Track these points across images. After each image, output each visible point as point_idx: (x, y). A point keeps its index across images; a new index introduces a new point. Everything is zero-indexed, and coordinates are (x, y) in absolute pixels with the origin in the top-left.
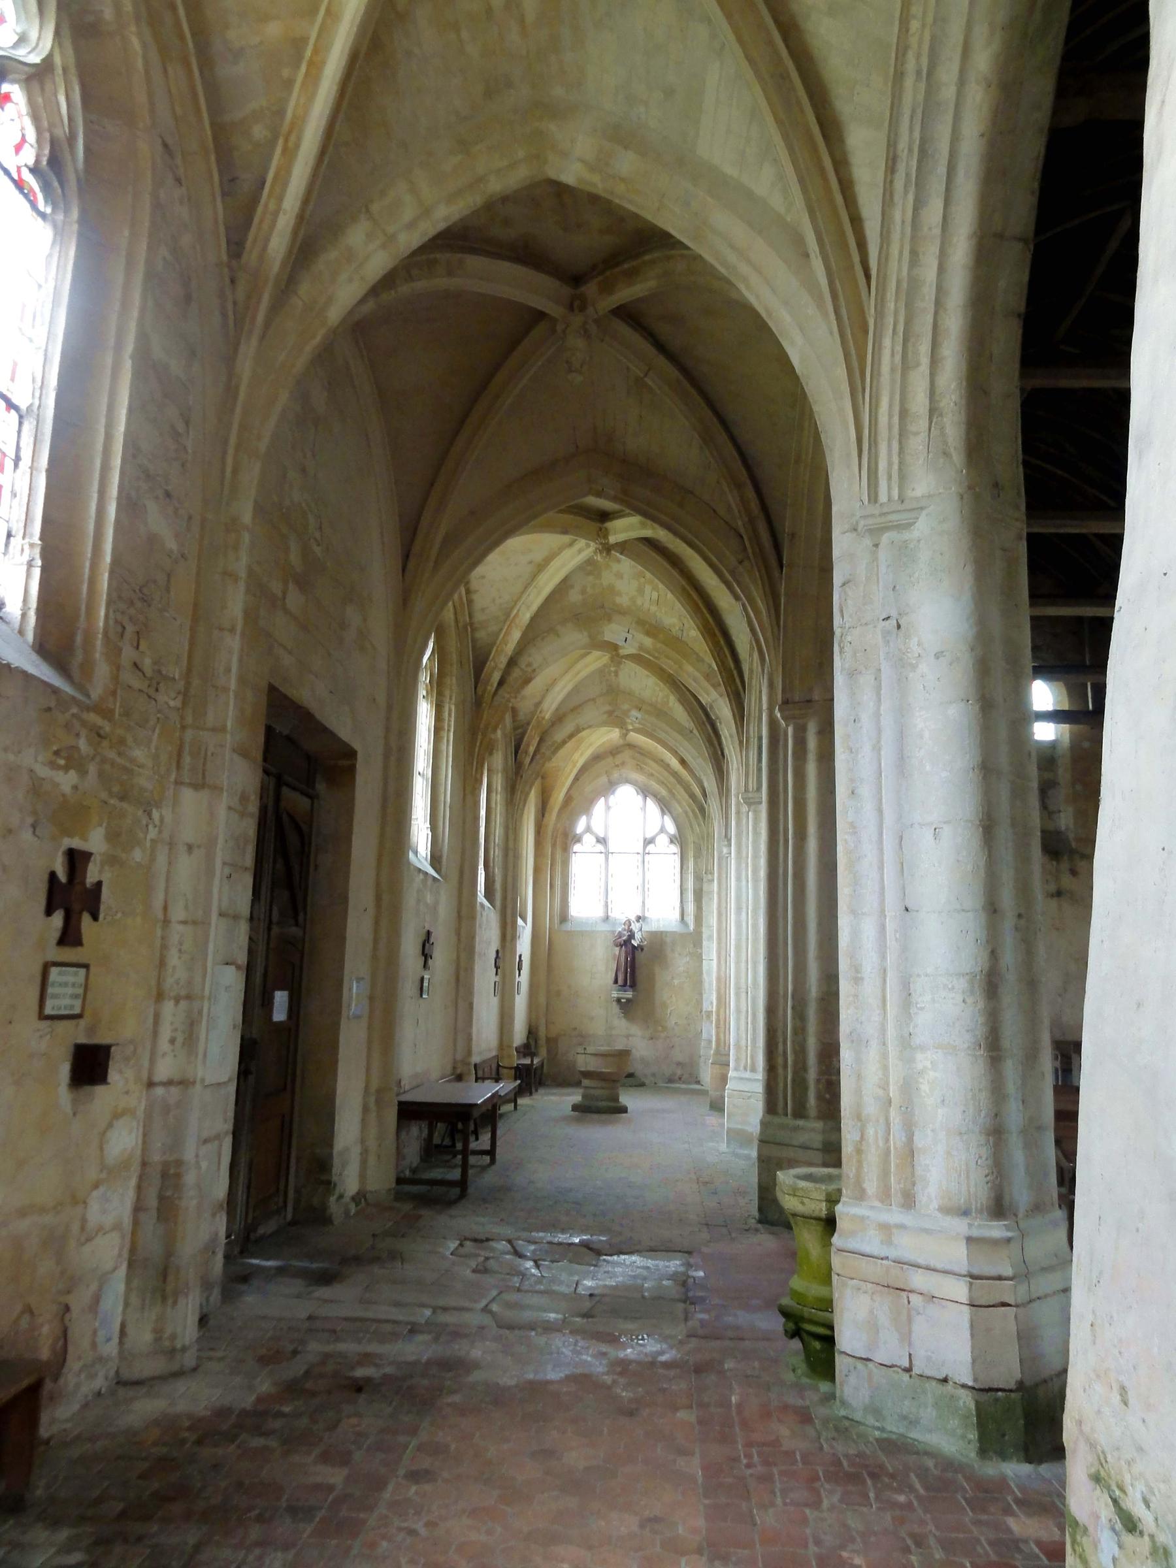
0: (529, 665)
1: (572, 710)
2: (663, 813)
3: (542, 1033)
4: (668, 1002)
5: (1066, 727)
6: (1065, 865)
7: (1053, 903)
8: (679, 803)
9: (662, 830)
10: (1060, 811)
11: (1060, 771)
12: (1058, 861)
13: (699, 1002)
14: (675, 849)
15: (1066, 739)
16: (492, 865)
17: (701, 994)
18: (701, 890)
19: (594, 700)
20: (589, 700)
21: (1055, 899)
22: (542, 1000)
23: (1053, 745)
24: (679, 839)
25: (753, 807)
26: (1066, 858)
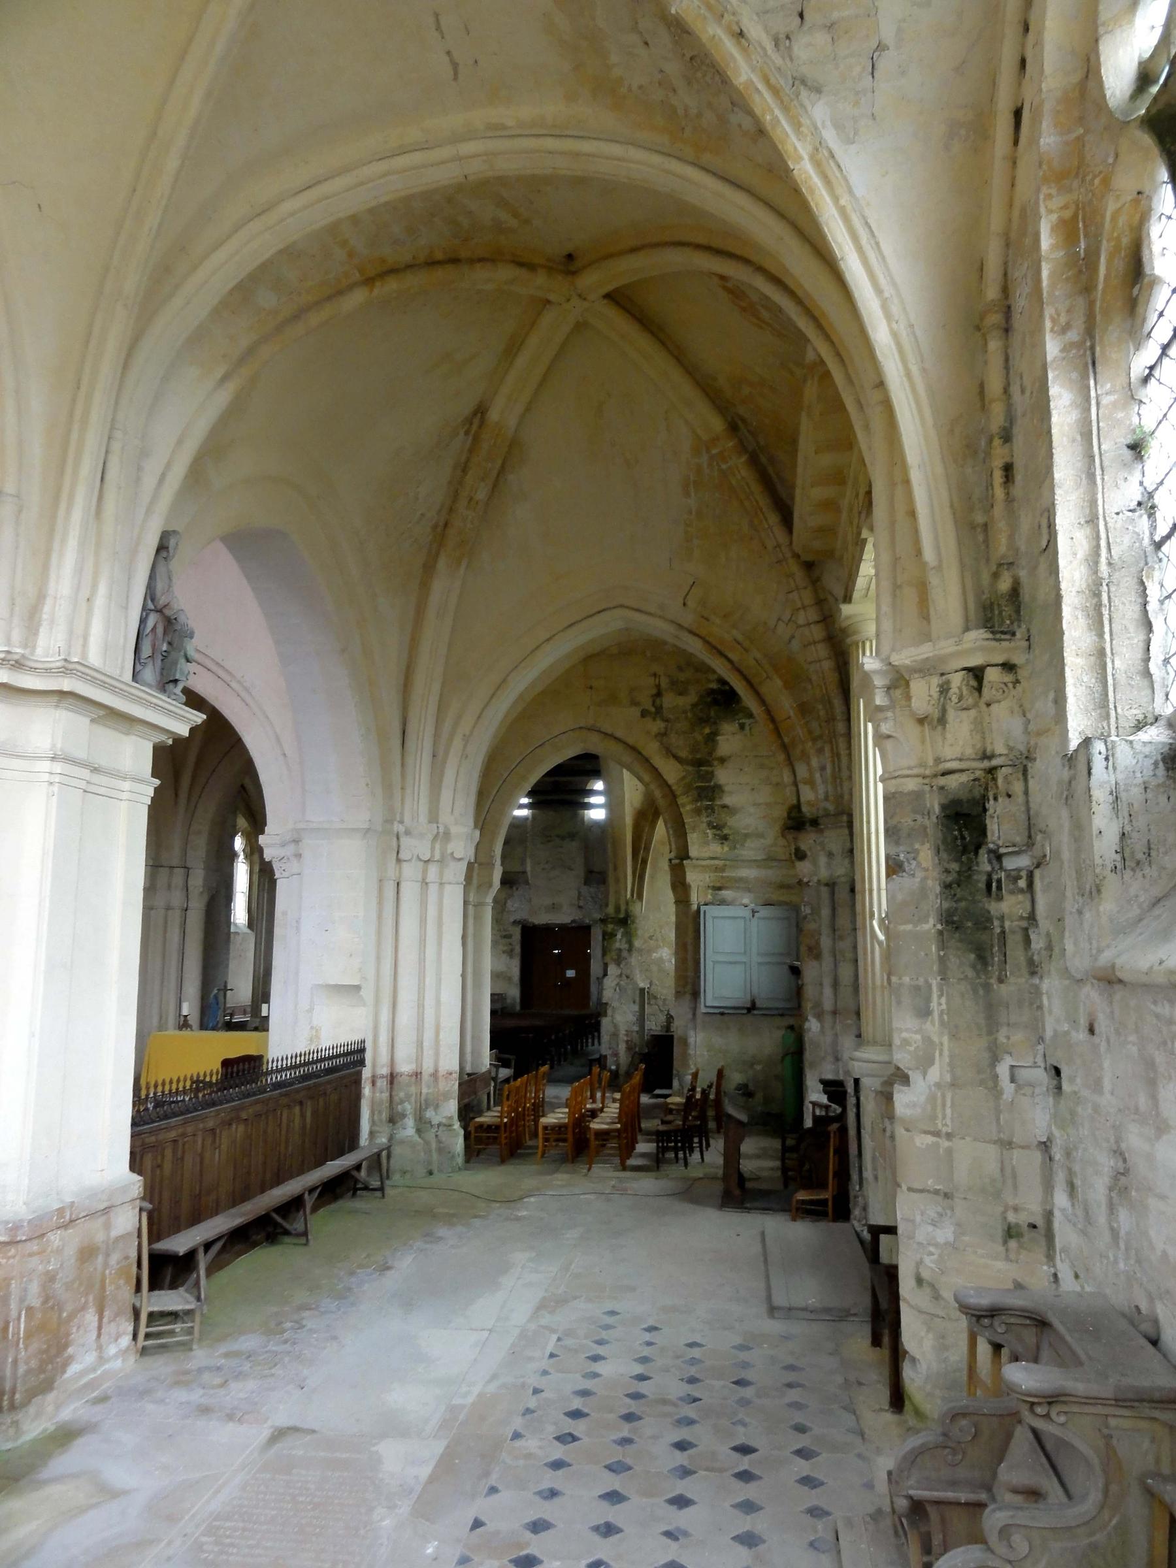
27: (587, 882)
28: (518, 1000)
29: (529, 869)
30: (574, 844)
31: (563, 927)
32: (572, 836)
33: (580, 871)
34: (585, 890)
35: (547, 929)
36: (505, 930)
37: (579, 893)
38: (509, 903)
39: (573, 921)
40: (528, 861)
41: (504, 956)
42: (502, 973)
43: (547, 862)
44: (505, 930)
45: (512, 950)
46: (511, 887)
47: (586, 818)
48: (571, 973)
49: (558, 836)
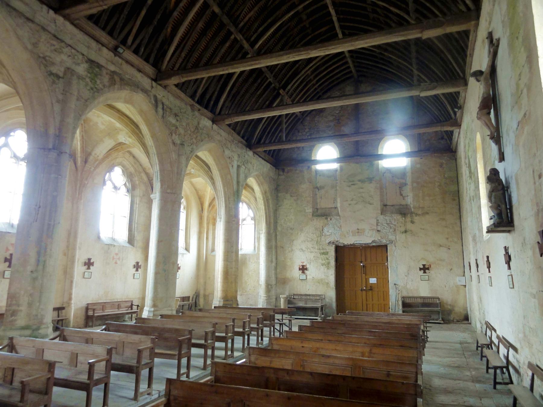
0: (96, 154)
2: (249, 208)
3: (202, 293)
4: (247, 281)
6: (409, 219)
8: (252, 204)
9: (248, 215)
10: (408, 196)
11: (408, 178)
12: (405, 217)
13: (258, 281)
14: (253, 222)
15: (410, 165)
16: (133, 230)
17: (259, 278)
18: (260, 237)
21: (404, 234)
22: (202, 281)
23: (405, 168)
24: (254, 219)
26: (409, 216)
27: (383, 212)
29: (339, 205)
31: (366, 248)
33: (377, 204)
35: (353, 248)
36: (323, 249)
37: (378, 220)
38: (325, 229)
39: (373, 242)
40: (339, 200)
41: (322, 268)
42: (322, 280)
43: (352, 200)
44: (323, 249)
45: (329, 263)
46: (326, 218)
47: (380, 166)
48: (373, 281)
49: (359, 181)
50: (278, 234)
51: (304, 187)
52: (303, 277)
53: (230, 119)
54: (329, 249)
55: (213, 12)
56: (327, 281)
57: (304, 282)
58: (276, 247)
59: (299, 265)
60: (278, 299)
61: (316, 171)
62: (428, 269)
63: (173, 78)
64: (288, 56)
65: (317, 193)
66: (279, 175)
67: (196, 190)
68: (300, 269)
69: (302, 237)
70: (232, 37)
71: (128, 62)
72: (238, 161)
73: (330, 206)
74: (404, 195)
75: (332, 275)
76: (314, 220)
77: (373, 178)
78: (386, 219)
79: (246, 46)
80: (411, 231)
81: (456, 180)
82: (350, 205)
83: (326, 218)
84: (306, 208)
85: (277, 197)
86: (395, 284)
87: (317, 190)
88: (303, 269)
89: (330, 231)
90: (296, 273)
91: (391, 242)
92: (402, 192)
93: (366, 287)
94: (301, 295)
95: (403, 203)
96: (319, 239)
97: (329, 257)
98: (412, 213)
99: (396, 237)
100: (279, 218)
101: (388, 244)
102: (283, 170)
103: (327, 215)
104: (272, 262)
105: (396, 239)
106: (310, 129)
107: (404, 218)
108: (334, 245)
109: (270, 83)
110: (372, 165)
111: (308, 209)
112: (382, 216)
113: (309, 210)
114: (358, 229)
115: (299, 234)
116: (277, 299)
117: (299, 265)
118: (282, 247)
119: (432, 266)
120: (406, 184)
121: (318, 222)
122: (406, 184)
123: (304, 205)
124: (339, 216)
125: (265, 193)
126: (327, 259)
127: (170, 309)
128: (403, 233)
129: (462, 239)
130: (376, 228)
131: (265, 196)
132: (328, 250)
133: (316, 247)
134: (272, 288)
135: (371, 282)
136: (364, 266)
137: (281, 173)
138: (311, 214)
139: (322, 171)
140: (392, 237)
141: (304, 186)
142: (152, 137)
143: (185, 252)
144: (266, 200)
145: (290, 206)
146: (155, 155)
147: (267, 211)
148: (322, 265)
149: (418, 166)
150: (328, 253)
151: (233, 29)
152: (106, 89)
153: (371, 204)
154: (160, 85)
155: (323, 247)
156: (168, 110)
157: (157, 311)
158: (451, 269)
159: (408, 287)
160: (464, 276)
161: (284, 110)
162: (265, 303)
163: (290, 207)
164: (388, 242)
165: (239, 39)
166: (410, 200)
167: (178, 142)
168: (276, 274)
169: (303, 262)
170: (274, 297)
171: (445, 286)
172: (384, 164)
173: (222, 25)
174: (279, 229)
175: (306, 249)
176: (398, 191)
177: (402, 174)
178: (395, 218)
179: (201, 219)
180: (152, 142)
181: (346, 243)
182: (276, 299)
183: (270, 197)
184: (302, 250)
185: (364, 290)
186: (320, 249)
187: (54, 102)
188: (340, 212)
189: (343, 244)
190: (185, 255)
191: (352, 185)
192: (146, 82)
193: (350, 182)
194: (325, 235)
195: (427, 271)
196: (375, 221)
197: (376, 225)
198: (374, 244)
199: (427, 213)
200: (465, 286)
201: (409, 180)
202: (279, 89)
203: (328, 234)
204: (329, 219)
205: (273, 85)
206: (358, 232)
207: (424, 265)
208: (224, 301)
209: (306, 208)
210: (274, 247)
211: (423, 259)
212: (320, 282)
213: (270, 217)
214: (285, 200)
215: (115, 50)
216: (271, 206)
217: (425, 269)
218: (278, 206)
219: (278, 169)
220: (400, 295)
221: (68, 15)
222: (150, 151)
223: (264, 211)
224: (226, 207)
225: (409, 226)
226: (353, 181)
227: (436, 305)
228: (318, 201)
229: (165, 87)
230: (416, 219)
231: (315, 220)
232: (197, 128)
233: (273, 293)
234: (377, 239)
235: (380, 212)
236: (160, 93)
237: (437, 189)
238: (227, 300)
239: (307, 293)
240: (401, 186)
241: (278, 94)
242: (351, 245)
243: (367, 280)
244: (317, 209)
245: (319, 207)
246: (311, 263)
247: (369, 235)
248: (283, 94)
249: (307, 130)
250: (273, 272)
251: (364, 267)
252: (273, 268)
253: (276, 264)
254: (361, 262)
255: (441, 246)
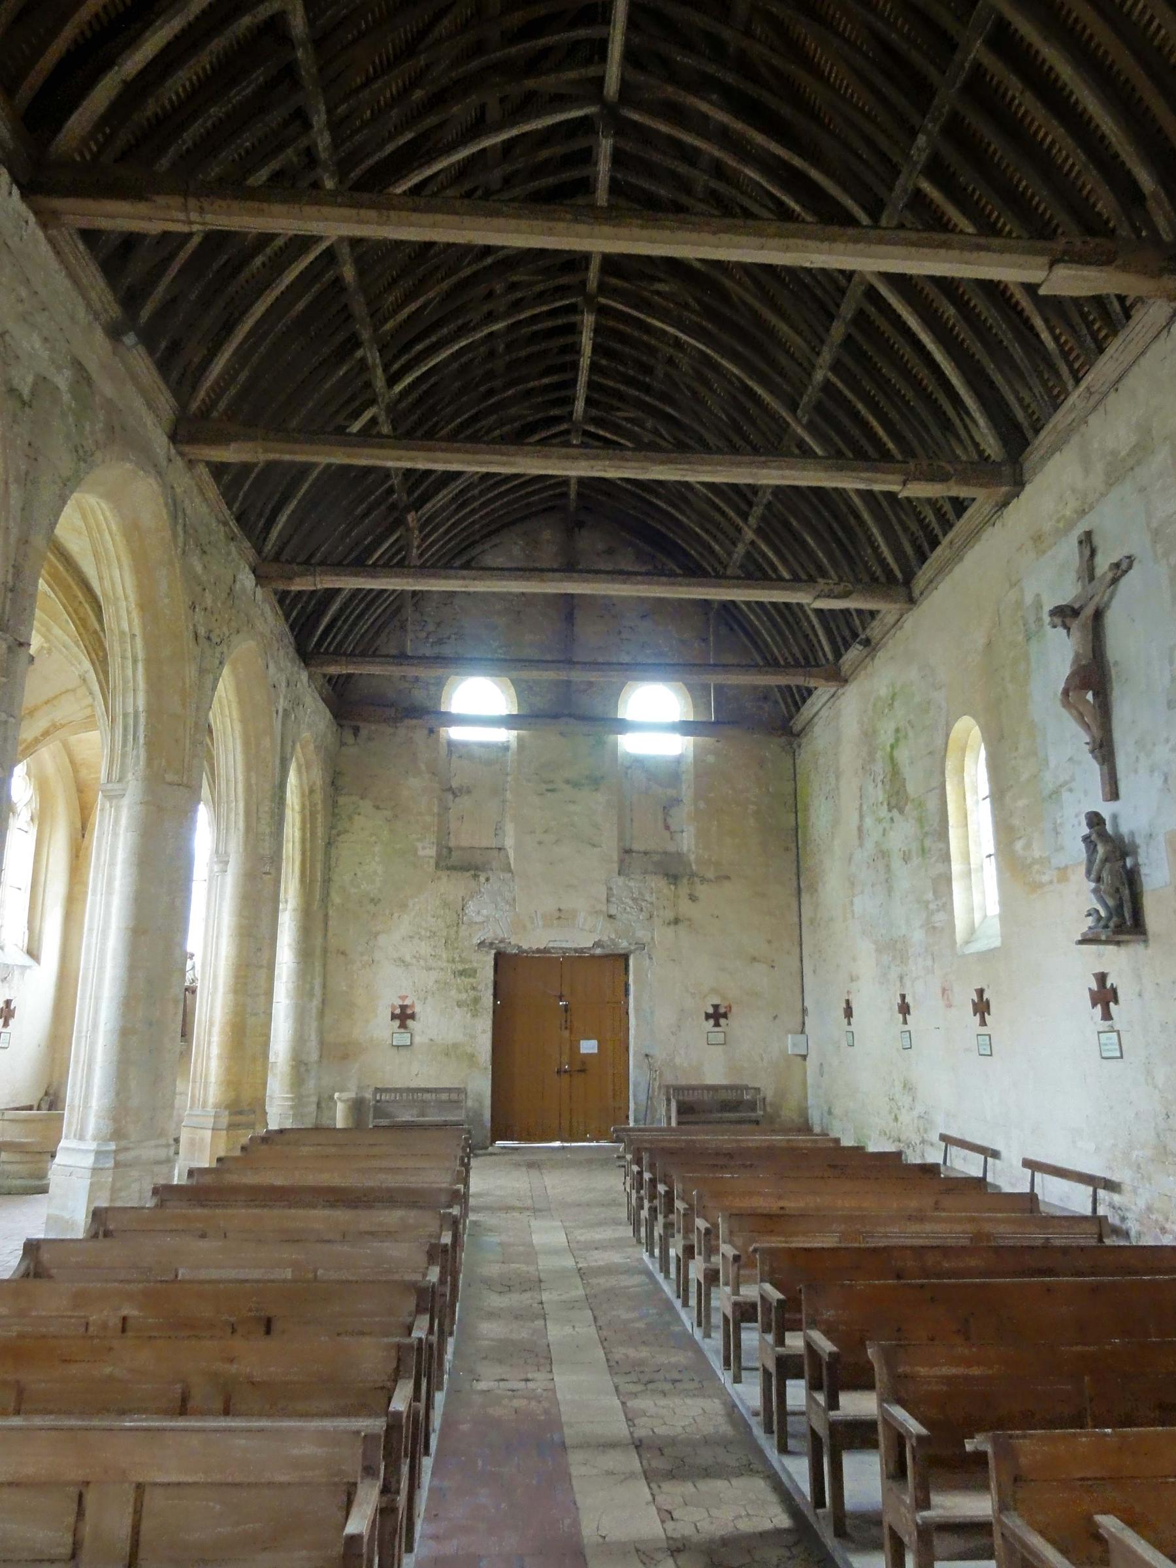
1: (46, 703)
5: (690, 740)
6: (684, 890)
7: (670, 931)
10: (682, 832)
11: (684, 787)
12: (675, 884)
19: (74, 690)
20: (67, 691)
21: (672, 927)
23: (678, 760)
25: (114, 802)
26: (685, 881)
28: (488, 1102)
29: (509, 842)
30: (601, 798)
31: (578, 960)
32: (595, 782)
33: (610, 845)
34: (620, 880)
35: (544, 960)
36: (462, 961)
38: (471, 907)
39: (597, 944)
40: (510, 828)
42: (455, 1046)
44: (462, 961)
45: (476, 1000)
46: (476, 876)
48: (589, 1047)
49: (567, 782)
50: (330, 913)
51: (415, 785)
52: (403, 1038)
53: (310, 579)
54: (478, 962)
55: (338, 280)
56: (469, 1050)
57: (403, 1052)
58: (325, 951)
59: (393, 1006)
60: (323, 1105)
61: (450, 744)
62: (725, 1016)
63: (233, 446)
64: (593, 463)
65: (451, 804)
66: (343, 744)
67: (72, 762)
68: (394, 1017)
69: (404, 925)
70: (359, 353)
71: (134, 378)
72: (285, 697)
73: (484, 844)
74: (673, 828)
75: (484, 1032)
76: (439, 878)
77: (602, 777)
78: (630, 888)
79: (380, 382)
80: (689, 920)
81: (791, 802)
82: (540, 843)
83: (476, 876)
84: (419, 845)
85: (335, 803)
86: (647, 1055)
87: (451, 797)
88: (403, 1016)
89: (485, 912)
90: (382, 1027)
91: (642, 946)
92: (670, 821)
93: (570, 1064)
94: (396, 1090)
95: (671, 848)
96: (452, 931)
97: (479, 984)
98: (693, 875)
99: (653, 934)
100: (337, 866)
101: (631, 952)
102: (356, 731)
103: (477, 868)
104: (311, 994)
105: (652, 938)
106: (438, 625)
107: (672, 887)
108: (493, 952)
109: (391, 491)
110: (601, 743)
111: (424, 848)
112: (622, 878)
113: (428, 851)
114: (560, 910)
115: (396, 915)
116: (324, 1103)
117: (393, 1006)
118: (343, 953)
119: (734, 1009)
120: (677, 801)
121: (452, 887)
122: (677, 801)
123: (414, 836)
124: (510, 871)
125: (312, 791)
126: (474, 988)
127: (163, 1141)
128: (669, 924)
129: (801, 945)
130: (604, 908)
131: (307, 803)
132: (475, 965)
133: (444, 956)
134: (307, 1071)
135: (583, 1051)
136: (566, 1008)
137: (350, 739)
138: (432, 862)
139: (465, 744)
140: (642, 934)
141: (415, 782)
142: (142, 607)
143: (27, 961)
144: (307, 813)
145: (372, 835)
146: (135, 661)
147: (308, 845)
148: (459, 1006)
149: (711, 759)
150: (475, 971)
151: (366, 335)
152: (99, 455)
153: (594, 846)
154: (181, 454)
155: (463, 955)
156: (191, 531)
157: (126, 1149)
158: (775, 1017)
159: (678, 1061)
160: (802, 1032)
161: (476, 582)
162: (287, 1118)
163: (374, 838)
164: (633, 948)
165: (370, 361)
166: (687, 842)
167: (202, 631)
168: (321, 1032)
169: (403, 998)
170: (314, 1099)
171: (762, 1059)
172: (630, 744)
173: (347, 316)
174: (336, 899)
175: (414, 961)
176: (660, 817)
177: (669, 773)
178: (653, 885)
179: (77, 856)
180: (136, 622)
181: (525, 947)
182: (319, 1104)
183: (319, 807)
184: (403, 962)
185: (566, 1072)
186: (453, 961)
187: (11, 480)
188: (512, 862)
189: (519, 947)
190: (28, 971)
191: (548, 790)
192: (160, 442)
193: (545, 782)
194: (471, 924)
195: (722, 1021)
196: (604, 890)
197: (605, 901)
198: (598, 951)
199: (728, 878)
200: (804, 1057)
201: (687, 792)
202: (406, 510)
203: (479, 919)
204: (482, 879)
205: (395, 496)
206: (559, 918)
207: (716, 1007)
208: (231, 1114)
209: (419, 845)
210: (318, 951)
211: (714, 991)
212: (451, 1051)
213: (313, 866)
214: (356, 817)
215: (115, 333)
216: (320, 831)
217: (717, 1016)
218: (334, 832)
219: (341, 726)
220: (657, 1084)
221: (55, 214)
222: (113, 645)
223: (298, 846)
224: (248, 828)
225: (686, 907)
226: (552, 782)
227: (752, 1106)
228: (453, 826)
229: (191, 464)
230: (702, 890)
231: (445, 879)
232: (231, 591)
233: (311, 1084)
234: (605, 938)
235: (615, 866)
236: (182, 480)
237: (752, 821)
238: (241, 1113)
239: (413, 1085)
240: (668, 806)
241: (400, 522)
242: (538, 951)
243: (574, 1048)
244: (450, 850)
245: (452, 843)
246: (426, 998)
247: (587, 927)
248: (411, 525)
249: (431, 627)
250: (314, 1025)
251: (566, 1011)
252: (314, 1011)
253: (323, 1002)
254: (561, 998)
255: (754, 959)
